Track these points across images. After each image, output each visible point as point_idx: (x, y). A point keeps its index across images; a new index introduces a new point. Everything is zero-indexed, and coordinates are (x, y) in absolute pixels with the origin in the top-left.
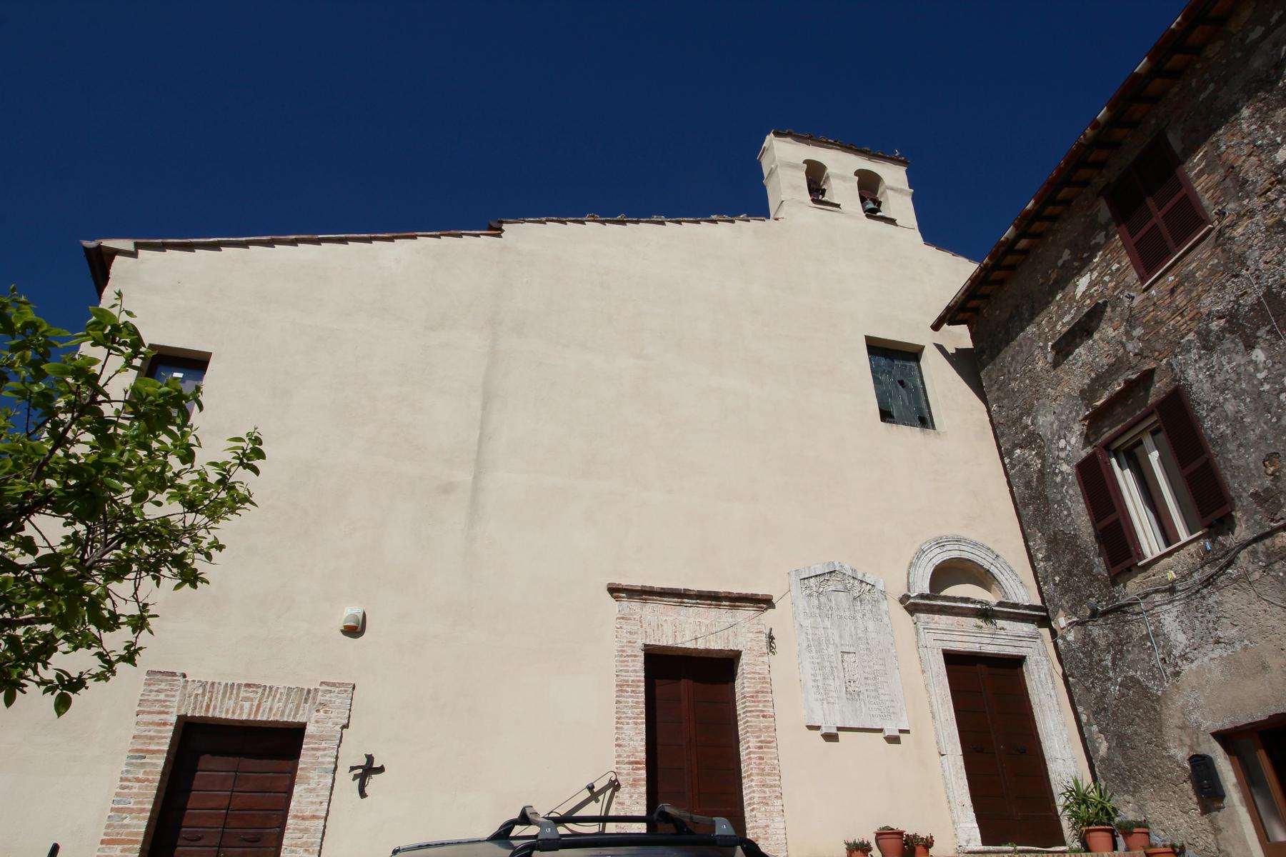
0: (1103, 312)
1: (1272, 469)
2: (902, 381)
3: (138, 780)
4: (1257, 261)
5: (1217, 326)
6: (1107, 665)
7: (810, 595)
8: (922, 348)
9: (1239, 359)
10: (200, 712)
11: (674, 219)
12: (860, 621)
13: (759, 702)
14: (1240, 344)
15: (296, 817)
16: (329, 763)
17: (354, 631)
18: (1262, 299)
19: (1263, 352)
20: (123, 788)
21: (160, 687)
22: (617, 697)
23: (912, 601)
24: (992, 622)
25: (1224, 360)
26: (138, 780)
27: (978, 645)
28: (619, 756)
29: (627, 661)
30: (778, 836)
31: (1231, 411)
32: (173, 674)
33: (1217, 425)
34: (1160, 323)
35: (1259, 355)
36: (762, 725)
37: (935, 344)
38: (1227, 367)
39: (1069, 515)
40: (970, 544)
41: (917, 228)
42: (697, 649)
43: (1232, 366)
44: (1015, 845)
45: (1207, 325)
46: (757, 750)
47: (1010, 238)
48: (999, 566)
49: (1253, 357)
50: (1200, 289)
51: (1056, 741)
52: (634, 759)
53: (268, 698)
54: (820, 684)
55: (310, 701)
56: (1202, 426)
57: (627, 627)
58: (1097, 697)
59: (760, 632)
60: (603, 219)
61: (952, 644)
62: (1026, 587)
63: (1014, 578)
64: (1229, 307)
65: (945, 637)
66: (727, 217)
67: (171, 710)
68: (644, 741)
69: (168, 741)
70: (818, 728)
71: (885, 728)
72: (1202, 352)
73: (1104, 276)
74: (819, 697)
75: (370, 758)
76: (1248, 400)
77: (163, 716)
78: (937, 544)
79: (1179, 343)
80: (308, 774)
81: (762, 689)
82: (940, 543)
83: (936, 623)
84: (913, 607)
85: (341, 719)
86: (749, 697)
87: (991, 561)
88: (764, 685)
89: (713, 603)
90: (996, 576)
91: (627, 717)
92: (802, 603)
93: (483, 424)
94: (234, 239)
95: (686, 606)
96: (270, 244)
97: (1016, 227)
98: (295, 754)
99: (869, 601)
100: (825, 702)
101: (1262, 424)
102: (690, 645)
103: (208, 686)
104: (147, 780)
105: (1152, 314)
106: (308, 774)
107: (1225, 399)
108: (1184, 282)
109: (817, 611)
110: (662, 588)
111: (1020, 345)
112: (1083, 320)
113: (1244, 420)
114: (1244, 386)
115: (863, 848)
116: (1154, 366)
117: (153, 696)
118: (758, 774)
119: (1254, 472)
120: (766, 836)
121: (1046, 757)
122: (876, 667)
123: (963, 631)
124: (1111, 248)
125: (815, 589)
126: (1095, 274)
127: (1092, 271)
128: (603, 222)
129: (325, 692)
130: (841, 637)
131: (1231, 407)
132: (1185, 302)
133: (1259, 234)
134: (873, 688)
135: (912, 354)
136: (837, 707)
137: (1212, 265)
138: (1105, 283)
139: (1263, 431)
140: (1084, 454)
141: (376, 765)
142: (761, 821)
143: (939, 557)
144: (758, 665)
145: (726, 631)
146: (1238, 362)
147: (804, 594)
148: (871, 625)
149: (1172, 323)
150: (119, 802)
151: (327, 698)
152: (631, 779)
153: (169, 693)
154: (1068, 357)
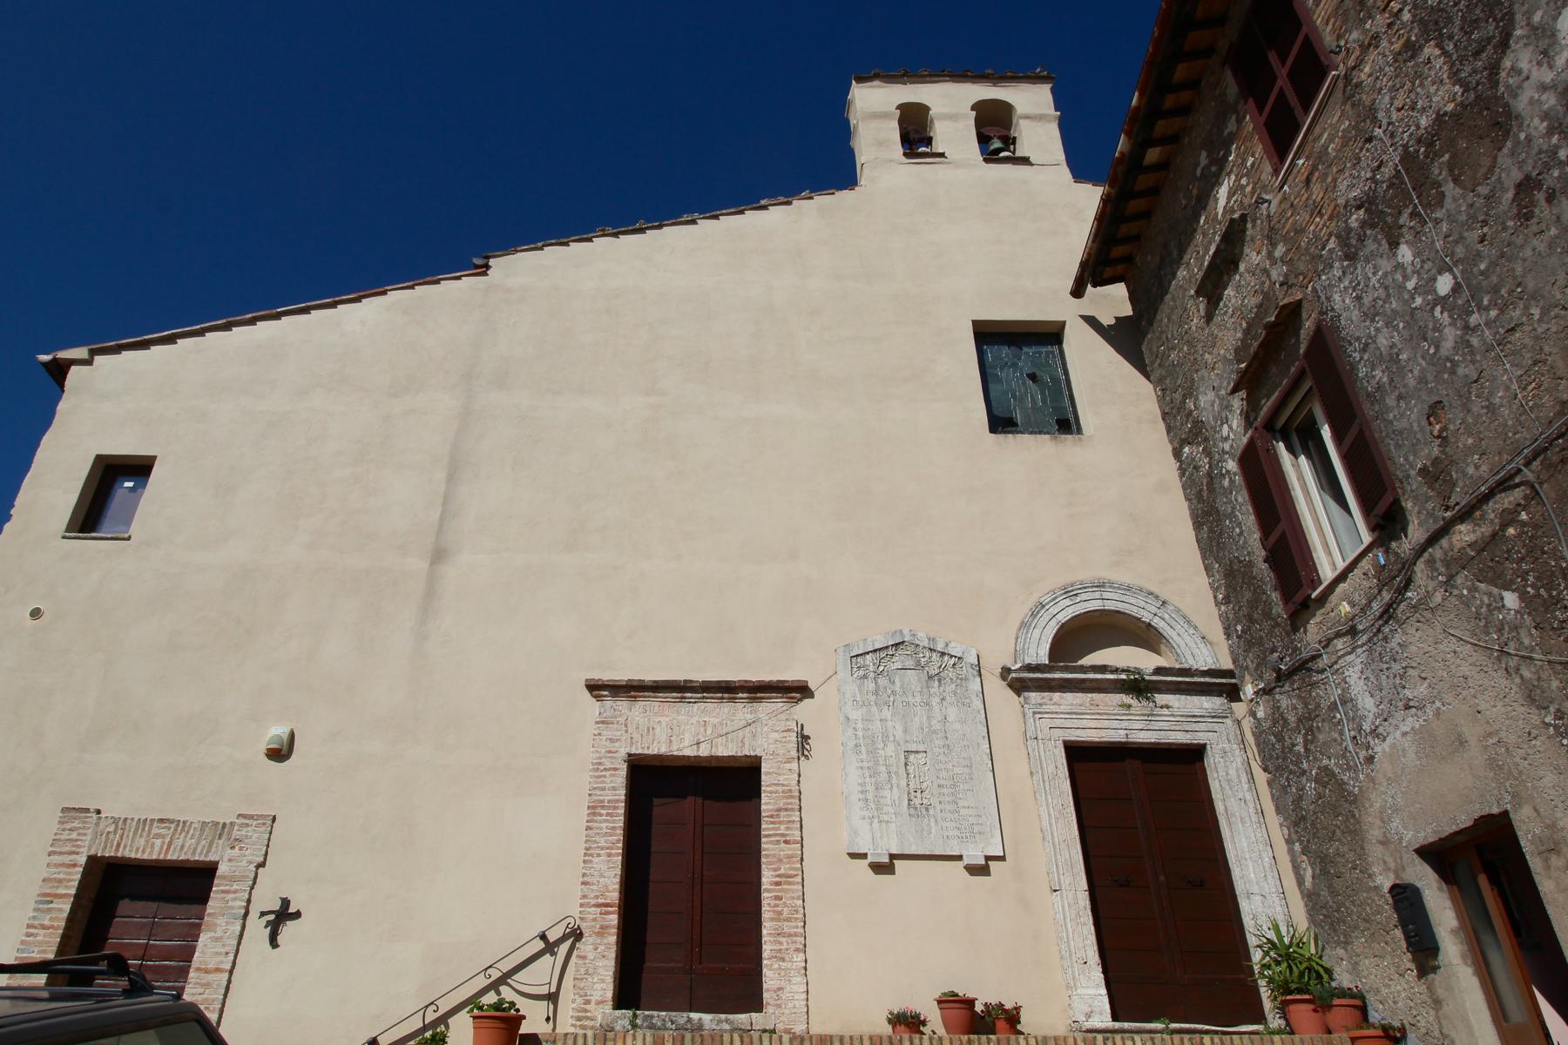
0: (1244, 231)
1: (1438, 427)
2: (1034, 373)
3: (43, 927)
4: (1388, 111)
5: (1356, 220)
6: (1299, 752)
7: (865, 677)
8: (1063, 324)
9: (1385, 265)
10: (110, 852)
11: (708, 215)
12: (936, 708)
13: (780, 823)
14: (1384, 242)
15: (198, 969)
16: (240, 907)
17: (279, 753)
18: (1400, 167)
19: (1409, 248)
20: (29, 935)
21: (73, 825)
22: (587, 821)
23: (1014, 675)
24: (1148, 699)
25: (1369, 270)
26: (43, 927)
27: (1123, 732)
28: (584, 897)
29: (605, 776)
30: (796, 1002)
31: (1385, 346)
32: (87, 810)
33: (1372, 370)
34: (1300, 231)
35: (1405, 253)
36: (782, 853)
37: (1082, 317)
38: (1374, 280)
39: (1241, 533)
40: (1120, 589)
41: (1064, 163)
42: (699, 757)
43: (1378, 277)
44: (1167, 1021)
45: (1346, 222)
46: (773, 887)
47: (1124, 150)
48: (1167, 616)
49: (1400, 260)
50: (1335, 170)
51: (1251, 868)
52: (603, 901)
53: (180, 834)
54: (870, 796)
55: (224, 837)
56: (1357, 375)
57: (607, 734)
58: (1294, 801)
59: (789, 730)
60: (614, 231)
61: (1079, 732)
62: (1210, 643)
63: (1192, 631)
64: (1367, 188)
65: (1068, 724)
66: (782, 199)
67: (82, 850)
68: (619, 877)
69: (76, 884)
70: (864, 856)
71: (965, 854)
72: (1345, 263)
73: (1241, 178)
74: (867, 814)
75: (286, 903)
76: (1401, 325)
77: (73, 857)
78: (1065, 593)
79: (1321, 256)
80: (216, 921)
81: (786, 807)
82: (1069, 592)
83: (1055, 704)
84: (1021, 682)
85: (257, 856)
86: (767, 817)
87: (1154, 610)
88: (789, 801)
89: (726, 695)
90: (1161, 631)
91: (599, 847)
92: (851, 688)
93: (446, 500)
94: (189, 329)
95: (690, 702)
96: (227, 327)
97: (1128, 134)
98: (204, 899)
99: (952, 679)
100: (876, 820)
101: (1420, 360)
102: (689, 752)
103: (120, 823)
104: (52, 927)
105: (1291, 220)
106: (216, 921)
107: (1377, 330)
108: (1318, 165)
109: (873, 698)
110: (655, 682)
111: (1173, 299)
112: (1222, 247)
113: (1400, 357)
114: (1394, 305)
115: (909, 1022)
116: (1300, 297)
117: (65, 836)
118: (772, 919)
119: (1418, 436)
120: (779, 1002)
121: (1237, 893)
122: (957, 770)
123: (1099, 714)
124: (1244, 135)
125: (872, 668)
126: (1233, 177)
127: (1229, 174)
128: (616, 235)
129: (242, 825)
130: (905, 731)
131: (1384, 342)
132: (1321, 195)
133: (1387, 69)
134: (950, 799)
135: (1051, 335)
136: (893, 827)
137: (1343, 131)
138: (1243, 188)
139: (1423, 370)
140: (1245, 440)
141: (292, 910)
142: (771, 982)
143: (1067, 611)
144: (784, 774)
145: (741, 732)
146: (1384, 270)
147: (855, 676)
148: (952, 713)
149: (1312, 228)
150: (23, 951)
151: (243, 833)
152: (598, 926)
153: (81, 831)
154: (1218, 305)
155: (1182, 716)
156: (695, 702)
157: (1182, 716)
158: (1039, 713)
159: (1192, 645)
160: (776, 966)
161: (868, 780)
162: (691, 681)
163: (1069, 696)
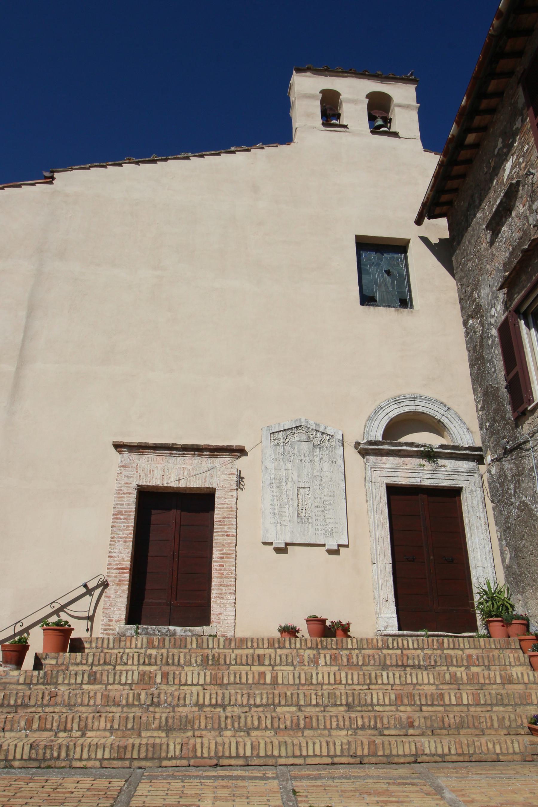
7: (278, 445)
12: (317, 464)
13: (225, 525)
22: (112, 522)
23: (362, 446)
24: (434, 462)
27: (419, 480)
28: (110, 564)
29: (123, 497)
36: (225, 542)
42: (179, 487)
48: (449, 416)
54: (276, 511)
57: (125, 473)
59: (232, 474)
63: (462, 425)
70: (271, 544)
74: (274, 521)
83: (384, 463)
88: (230, 513)
89: (196, 453)
90: (446, 424)
92: (269, 451)
100: (279, 524)
102: (174, 485)
109: (282, 457)
110: (154, 444)
118: (217, 577)
122: (326, 498)
123: (407, 469)
125: (282, 440)
130: (299, 476)
134: (321, 514)
136: (288, 528)
144: (228, 498)
145: (204, 474)
147: (272, 444)
148: (326, 466)
152: (118, 580)
155: (452, 471)
156: (178, 457)
157: (452, 471)
158: (374, 468)
159: (461, 433)
160: (219, 602)
161: (276, 502)
162: (176, 444)
163: (391, 459)
